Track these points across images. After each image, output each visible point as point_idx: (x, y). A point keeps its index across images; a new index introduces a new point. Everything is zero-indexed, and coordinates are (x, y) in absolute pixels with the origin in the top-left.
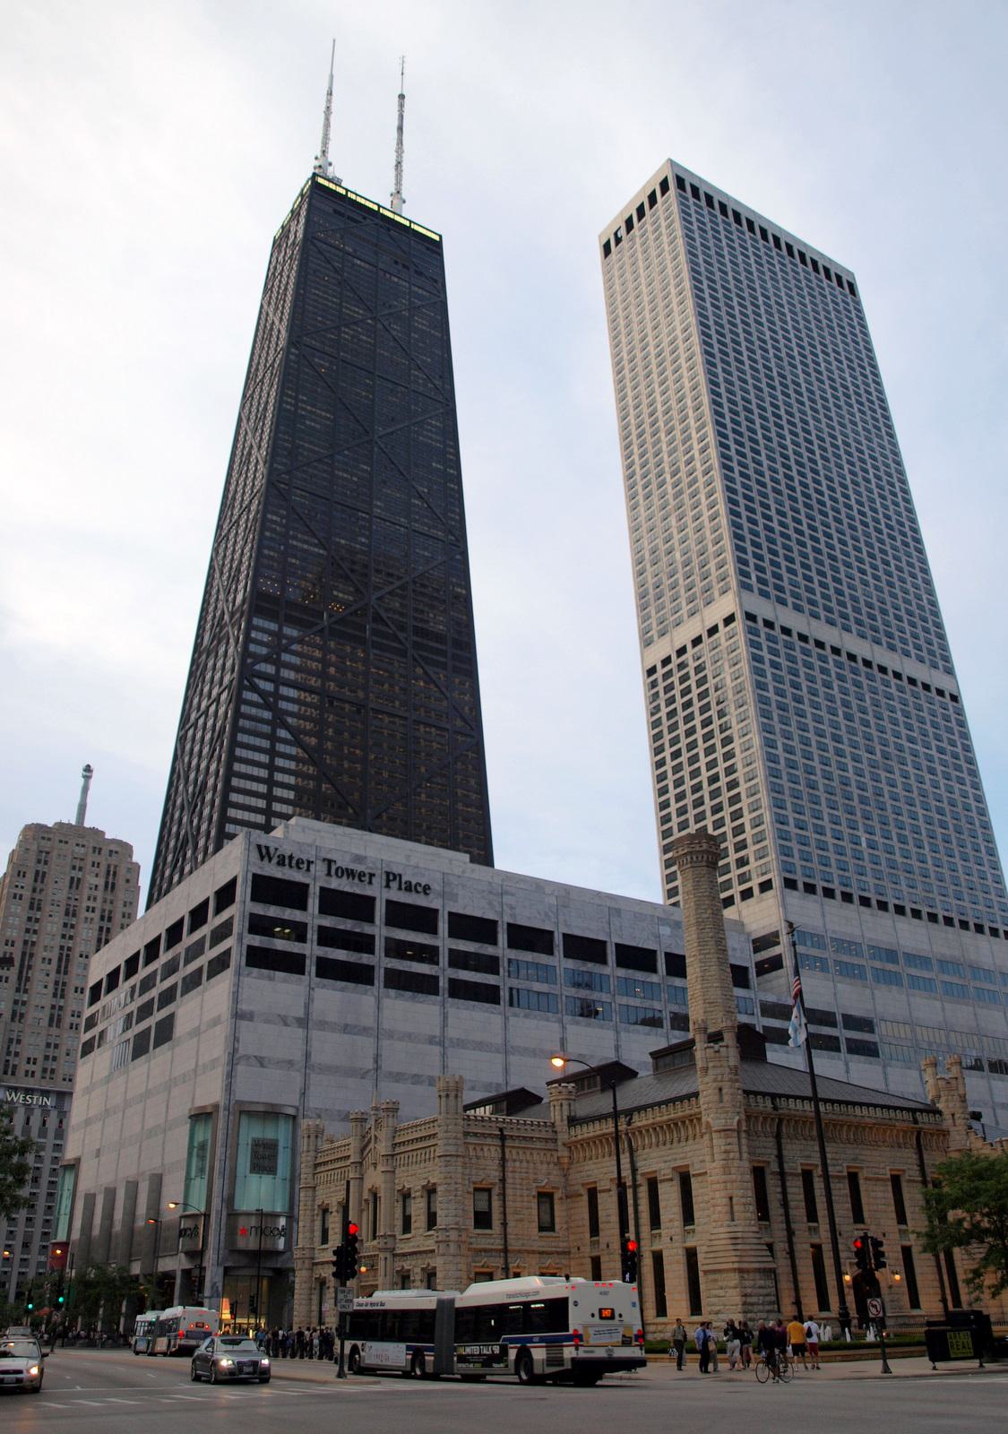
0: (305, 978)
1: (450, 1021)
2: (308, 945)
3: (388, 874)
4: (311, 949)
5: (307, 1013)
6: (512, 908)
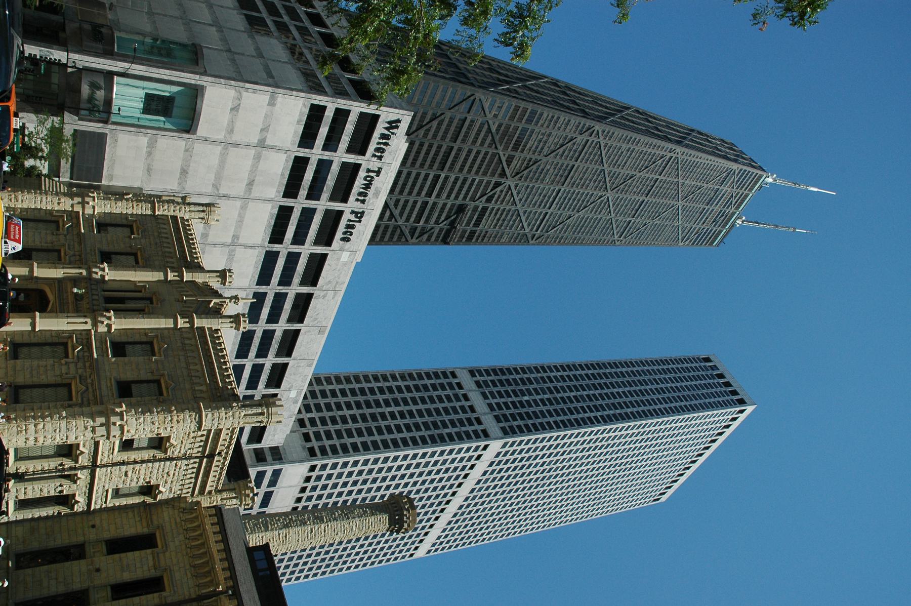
0: (295, 148)
1: (250, 251)
2: (320, 152)
3: (363, 213)
4: (316, 153)
5: (268, 147)
6: (324, 297)
